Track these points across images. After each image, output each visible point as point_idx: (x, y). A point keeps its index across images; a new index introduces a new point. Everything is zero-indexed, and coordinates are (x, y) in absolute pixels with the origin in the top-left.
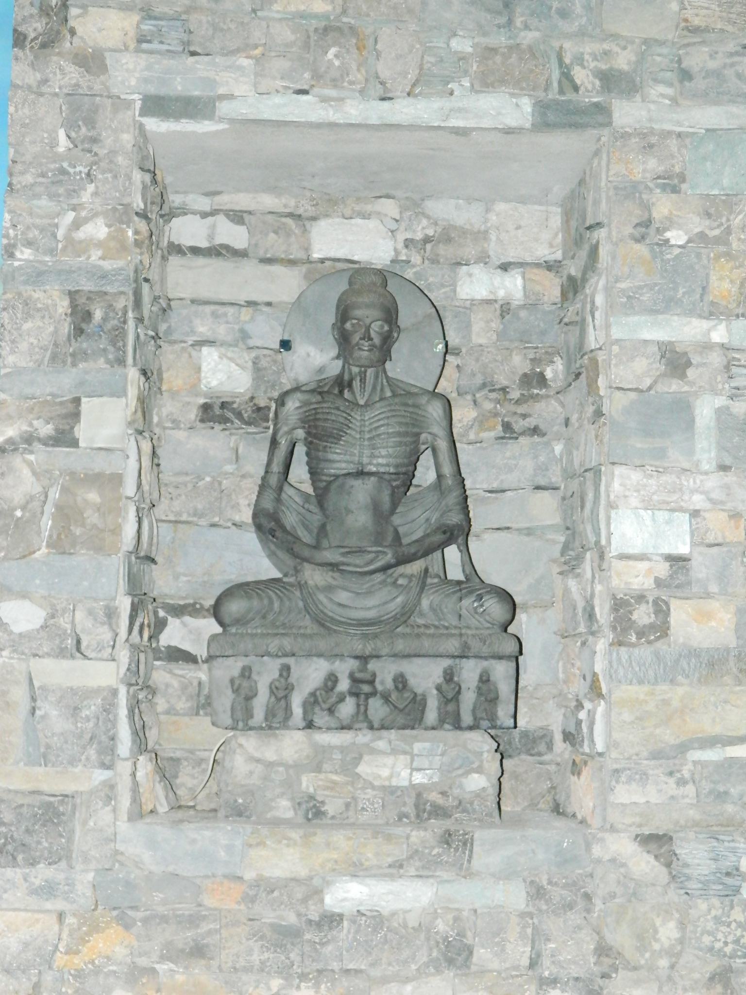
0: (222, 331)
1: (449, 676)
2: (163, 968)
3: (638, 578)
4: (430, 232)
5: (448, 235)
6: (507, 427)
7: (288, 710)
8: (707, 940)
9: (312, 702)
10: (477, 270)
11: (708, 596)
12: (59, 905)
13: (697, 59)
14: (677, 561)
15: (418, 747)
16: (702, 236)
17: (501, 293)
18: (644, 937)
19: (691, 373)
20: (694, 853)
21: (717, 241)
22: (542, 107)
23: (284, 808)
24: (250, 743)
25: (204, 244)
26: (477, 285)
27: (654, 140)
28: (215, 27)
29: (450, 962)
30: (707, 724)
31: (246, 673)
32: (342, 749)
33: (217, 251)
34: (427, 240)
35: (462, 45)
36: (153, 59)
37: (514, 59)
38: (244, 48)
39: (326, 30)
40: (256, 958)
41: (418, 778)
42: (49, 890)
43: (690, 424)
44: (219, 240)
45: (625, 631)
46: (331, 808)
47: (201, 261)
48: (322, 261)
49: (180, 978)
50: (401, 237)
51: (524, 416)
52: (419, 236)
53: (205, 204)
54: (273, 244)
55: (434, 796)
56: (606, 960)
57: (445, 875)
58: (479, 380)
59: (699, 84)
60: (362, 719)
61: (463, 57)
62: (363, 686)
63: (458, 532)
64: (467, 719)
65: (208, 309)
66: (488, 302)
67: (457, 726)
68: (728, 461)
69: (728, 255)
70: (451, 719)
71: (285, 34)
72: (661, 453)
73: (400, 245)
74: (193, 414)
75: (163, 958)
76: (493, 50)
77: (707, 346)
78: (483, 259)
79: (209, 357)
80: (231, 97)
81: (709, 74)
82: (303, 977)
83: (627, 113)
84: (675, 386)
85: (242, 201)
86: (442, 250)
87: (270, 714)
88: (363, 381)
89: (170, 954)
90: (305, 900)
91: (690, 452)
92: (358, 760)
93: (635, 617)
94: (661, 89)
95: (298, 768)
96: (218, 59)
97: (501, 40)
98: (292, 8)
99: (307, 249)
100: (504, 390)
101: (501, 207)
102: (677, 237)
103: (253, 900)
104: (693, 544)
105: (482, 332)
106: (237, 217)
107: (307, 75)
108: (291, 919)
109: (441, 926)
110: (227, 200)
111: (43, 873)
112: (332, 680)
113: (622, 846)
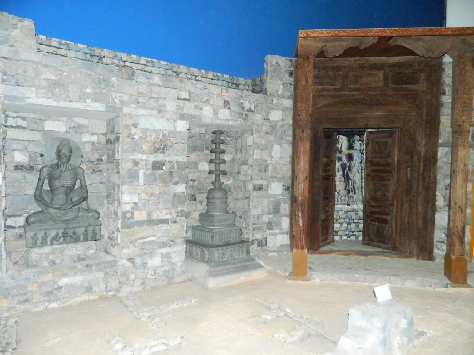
0: (20, 147)
1: (86, 231)
3: (127, 207)
4: (75, 125)
5: (79, 126)
6: (94, 170)
7: (46, 242)
8: (140, 276)
10: (86, 135)
11: (141, 210)
13: (141, 99)
14: (135, 204)
15: (78, 246)
16: (141, 137)
17: (92, 140)
19: (139, 166)
20: (138, 261)
21: (144, 138)
22: (108, 107)
23: (46, 264)
24: (36, 250)
25: (14, 125)
26: (86, 138)
27: (132, 116)
28: (25, 79)
29: (88, 291)
30: (141, 235)
31: (35, 235)
32: (60, 248)
33: (18, 127)
34: (74, 127)
35: (89, 91)
36: (6, 86)
37: (101, 96)
38: (33, 86)
39: (55, 84)
40: (42, 299)
41: (78, 252)
43: (138, 176)
44: (18, 124)
45: (125, 219)
46: (58, 262)
47: (14, 129)
48: (47, 131)
49: (22, 307)
50: (68, 126)
51: (98, 168)
52: (72, 126)
53: (14, 115)
54: (34, 126)
55: (82, 256)
56: (121, 285)
57: (86, 273)
58: (87, 160)
59: (141, 105)
60: (65, 242)
61: (89, 94)
62: (65, 235)
63: (85, 198)
64: (89, 239)
65: (16, 142)
66: (89, 142)
68: (146, 183)
69: (146, 141)
71: (44, 83)
72: (132, 182)
73: (68, 128)
75: (17, 304)
76: (96, 93)
77: (142, 160)
78: (88, 132)
79: (17, 154)
80: (29, 98)
81: (143, 103)
82: (54, 301)
83: (126, 110)
84: (136, 168)
85: (25, 115)
86: (78, 130)
87: (42, 243)
88: (63, 165)
89: (19, 303)
90: (53, 285)
91: (138, 181)
92: (64, 250)
93: (127, 216)
94: (134, 105)
95: (49, 254)
96: (26, 88)
97: (98, 91)
98: (46, 77)
99: (43, 128)
100: (93, 162)
101: (92, 120)
102: (136, 137)
103: (40, 287)
104: (139, 200)
105: (87, 149)
106: (23, 119)
107: (50, 94)
108: (49, 289)
109: (86, 284)
110: (21, 114)
112: (57, 234)
113: (125, 262)
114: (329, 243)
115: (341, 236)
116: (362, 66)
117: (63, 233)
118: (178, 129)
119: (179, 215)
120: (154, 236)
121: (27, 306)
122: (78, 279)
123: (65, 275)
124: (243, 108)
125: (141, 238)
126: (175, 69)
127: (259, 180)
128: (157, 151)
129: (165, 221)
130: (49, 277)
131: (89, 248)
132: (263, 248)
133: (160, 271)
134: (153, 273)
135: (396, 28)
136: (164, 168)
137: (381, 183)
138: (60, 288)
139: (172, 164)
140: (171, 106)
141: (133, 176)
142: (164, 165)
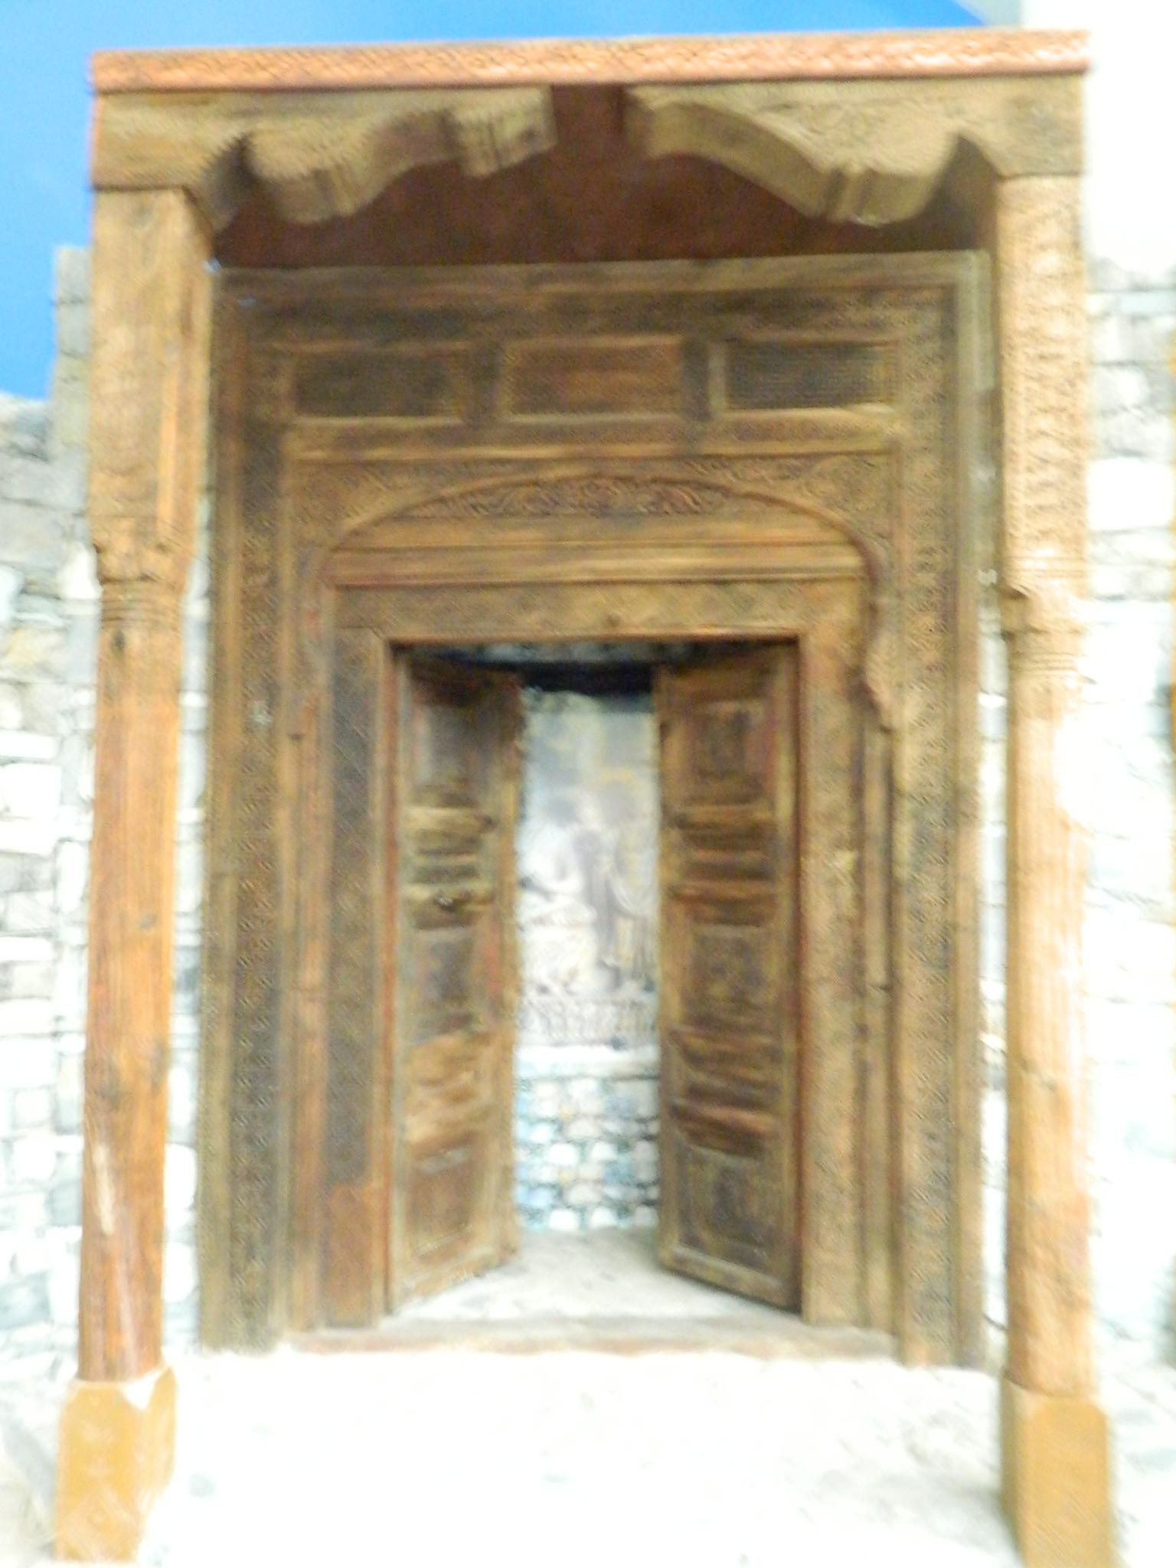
114: (481, 1269)
115: (582, 1210)
116: (570, 313)
132: (22, 1335)
135: (638, 39)
137: (728, 932)
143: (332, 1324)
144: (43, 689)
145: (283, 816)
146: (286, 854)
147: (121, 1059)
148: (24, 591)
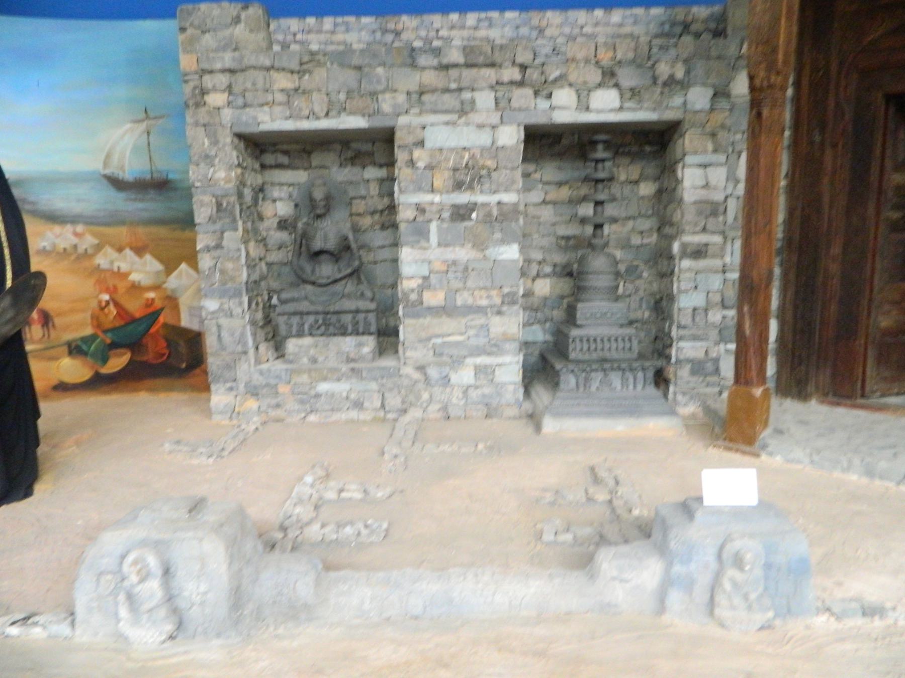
2: (270, 410)
7: (303, 331)
9: (311, 327)
11: (435, 289)
12: (234, 393)
18: (418, 397)
20: (433, 373)
41: (347, 349)
42: (231, 389)
46: (321, 359)
64: (361, 330)
67: (358, 334)
70: (356, 333)
72: (418, 242)
74: (275, 225)
77: (432, 203)
80: (263, 122)
85: (285, 147)
91: (428, 240)
111: (228, 385)
113: (408, 370)
117: (324, 320)
118: (500, 143)
119: (506, 300)
120: (461, 334)
121: (279, 413)
122: (342, 387)
123: (325, 379)
124: (655, 80)
125: (438, 336)
126: (535, 22)
127: (694, 233)
128: (458, 186)
129: (480, 310)
130: (305, 378)
131: (360, 345)
132: (709, 379)
133: (474, 394)
134: (461, 395)
136: (474, 215)
138: (318, 396)
139: (488, 209)
140: (485, 99)
141: (422, 233)
142: (473, 210)
143: (835, 395)
144: (722, 135)
145: (826, 180)
146: (826, 199)
147: (755, 273)
148: (715, 95)
